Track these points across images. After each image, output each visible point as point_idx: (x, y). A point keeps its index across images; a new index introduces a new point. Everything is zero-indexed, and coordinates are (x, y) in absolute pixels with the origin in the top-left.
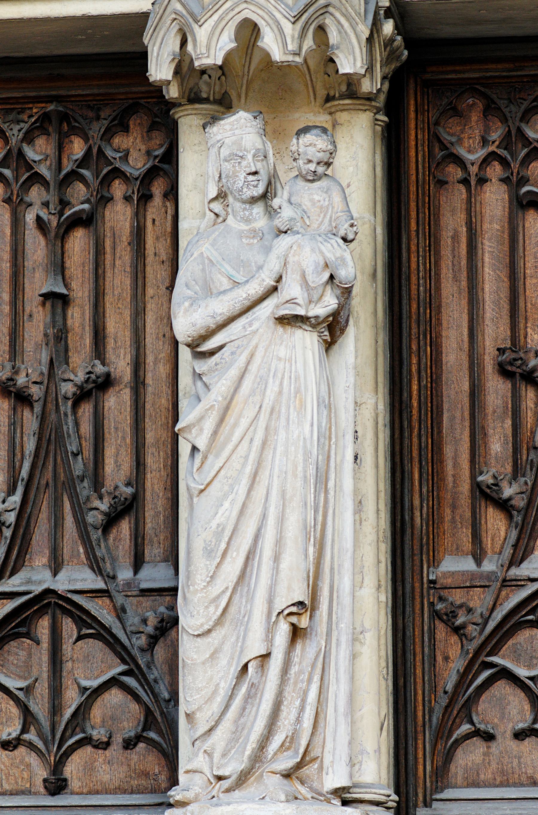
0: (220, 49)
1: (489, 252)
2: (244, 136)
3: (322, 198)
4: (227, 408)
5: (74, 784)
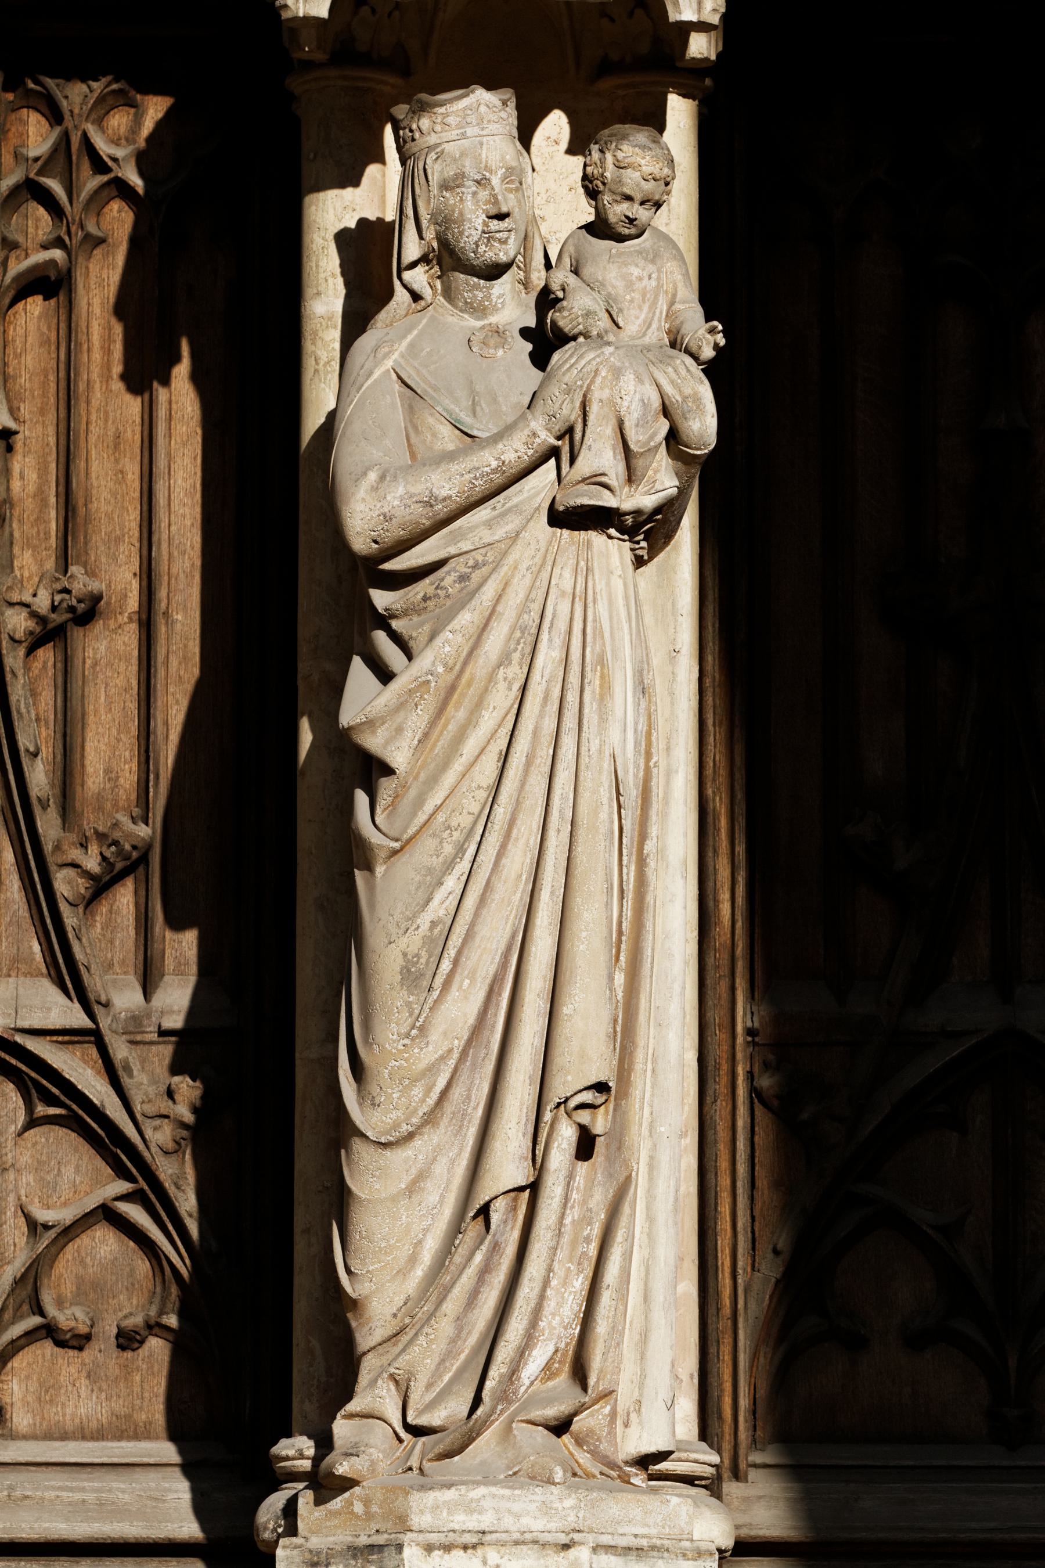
2: (485, 139)
3: (645, 274)
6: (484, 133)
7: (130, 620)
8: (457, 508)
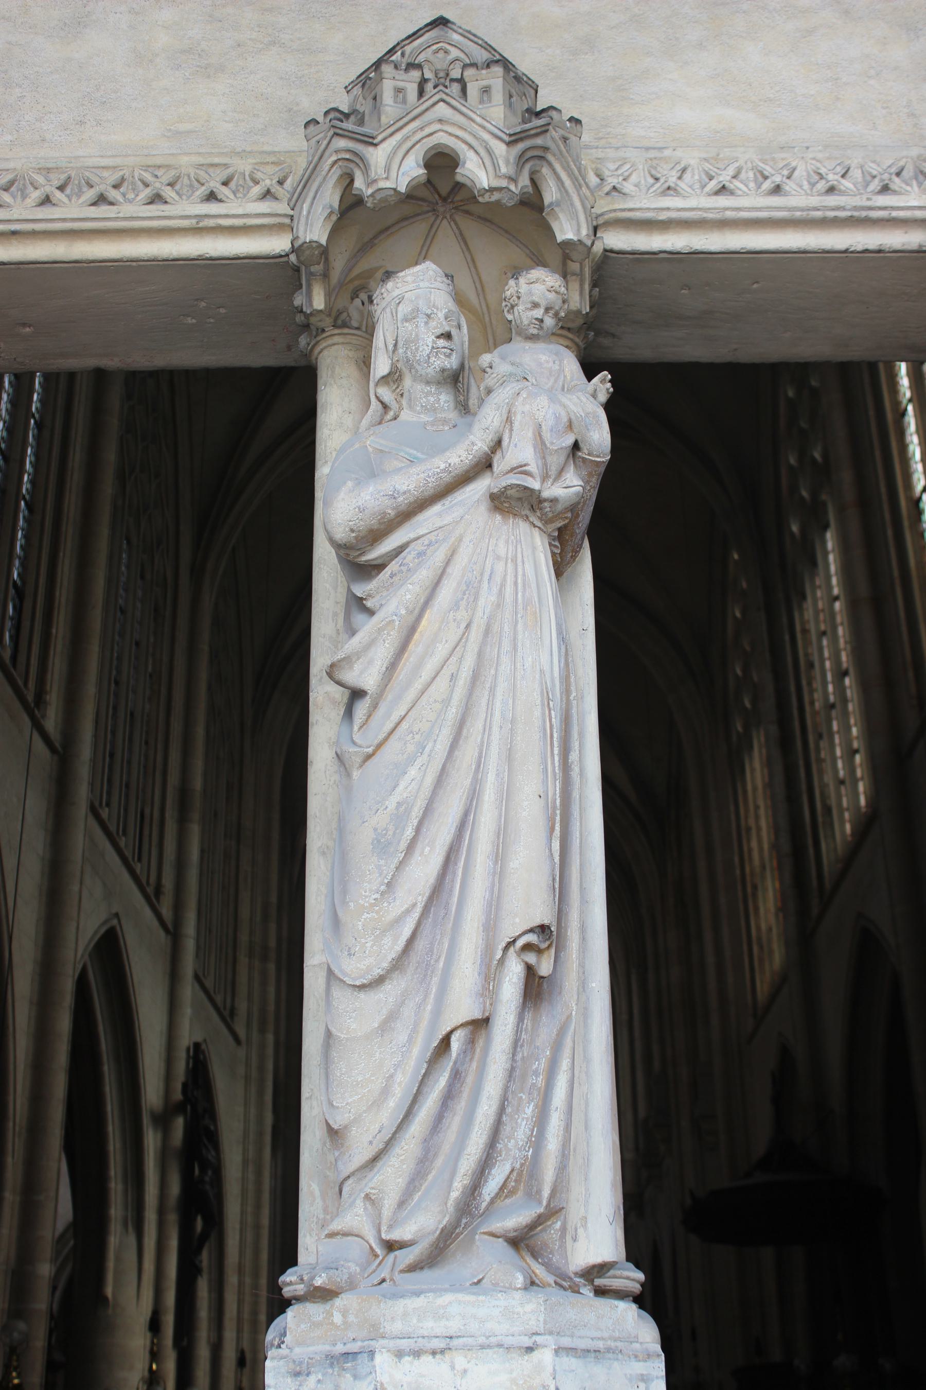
4: (412, 630)
6: (432, 286)
8: (415, 501)
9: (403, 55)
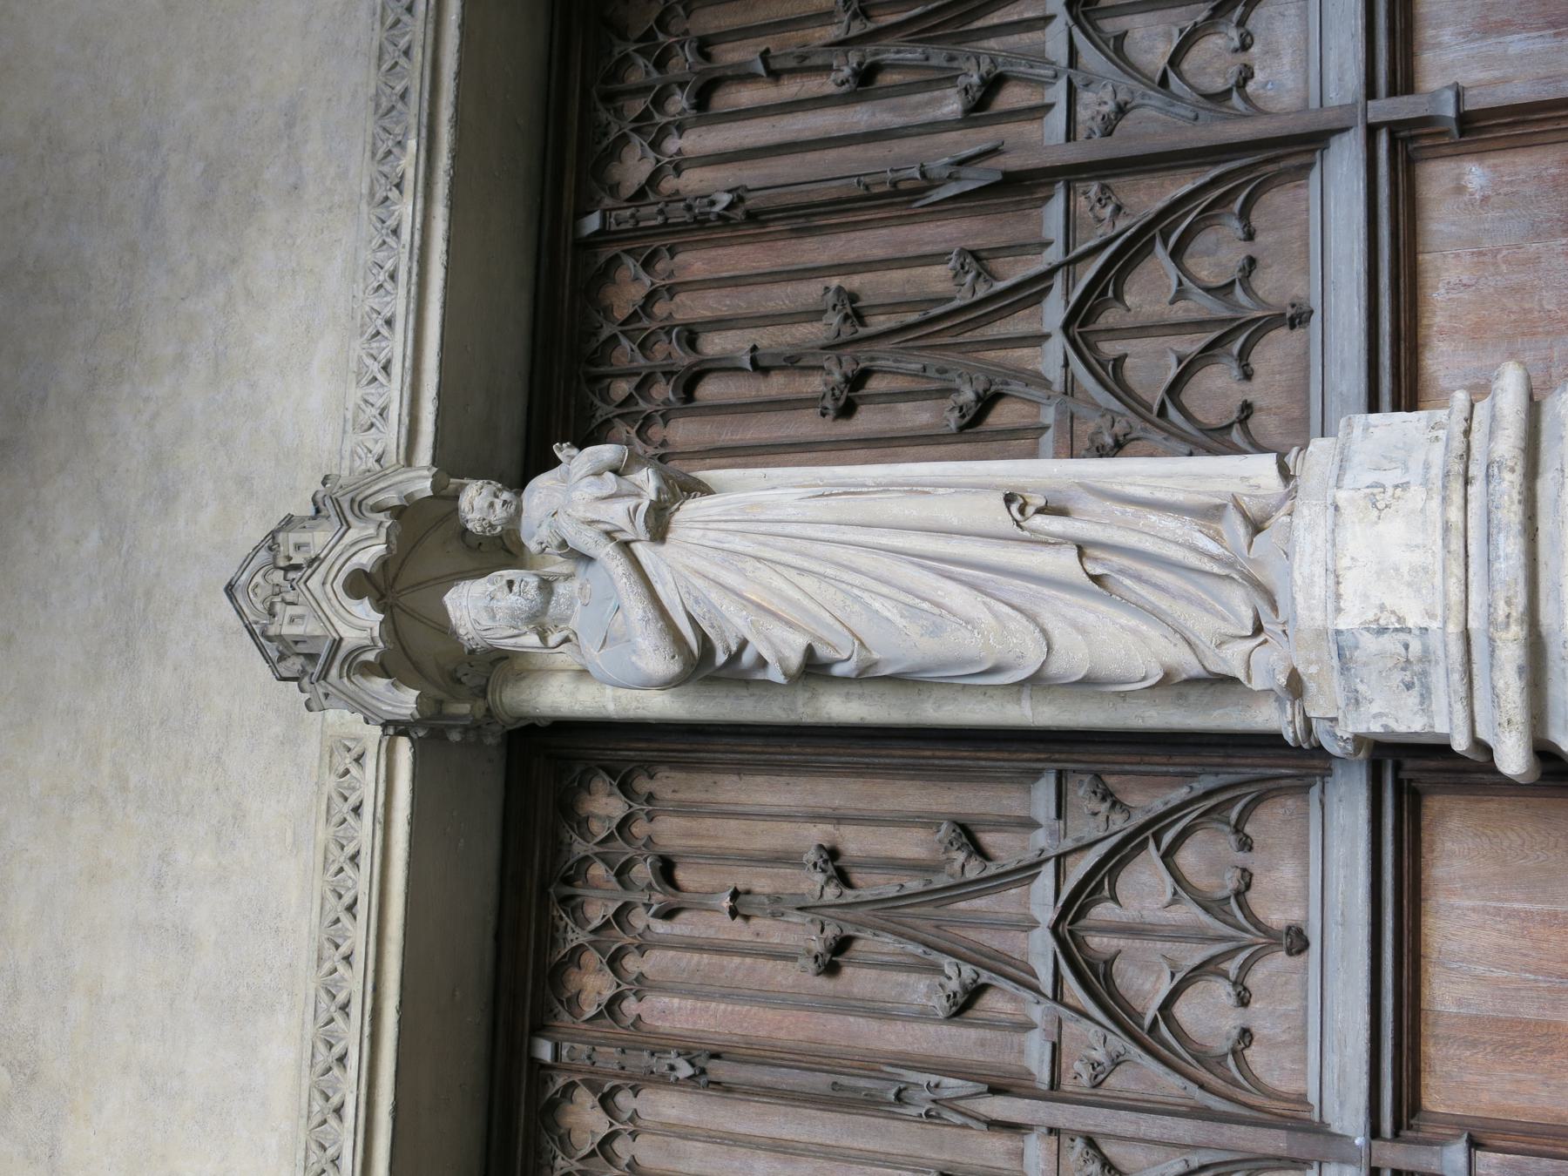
0: (367, 616)
1: (732, 435)
4: (759, 607)
5: (1294, 915)
7: (838, 829)
9: (256, 623)
